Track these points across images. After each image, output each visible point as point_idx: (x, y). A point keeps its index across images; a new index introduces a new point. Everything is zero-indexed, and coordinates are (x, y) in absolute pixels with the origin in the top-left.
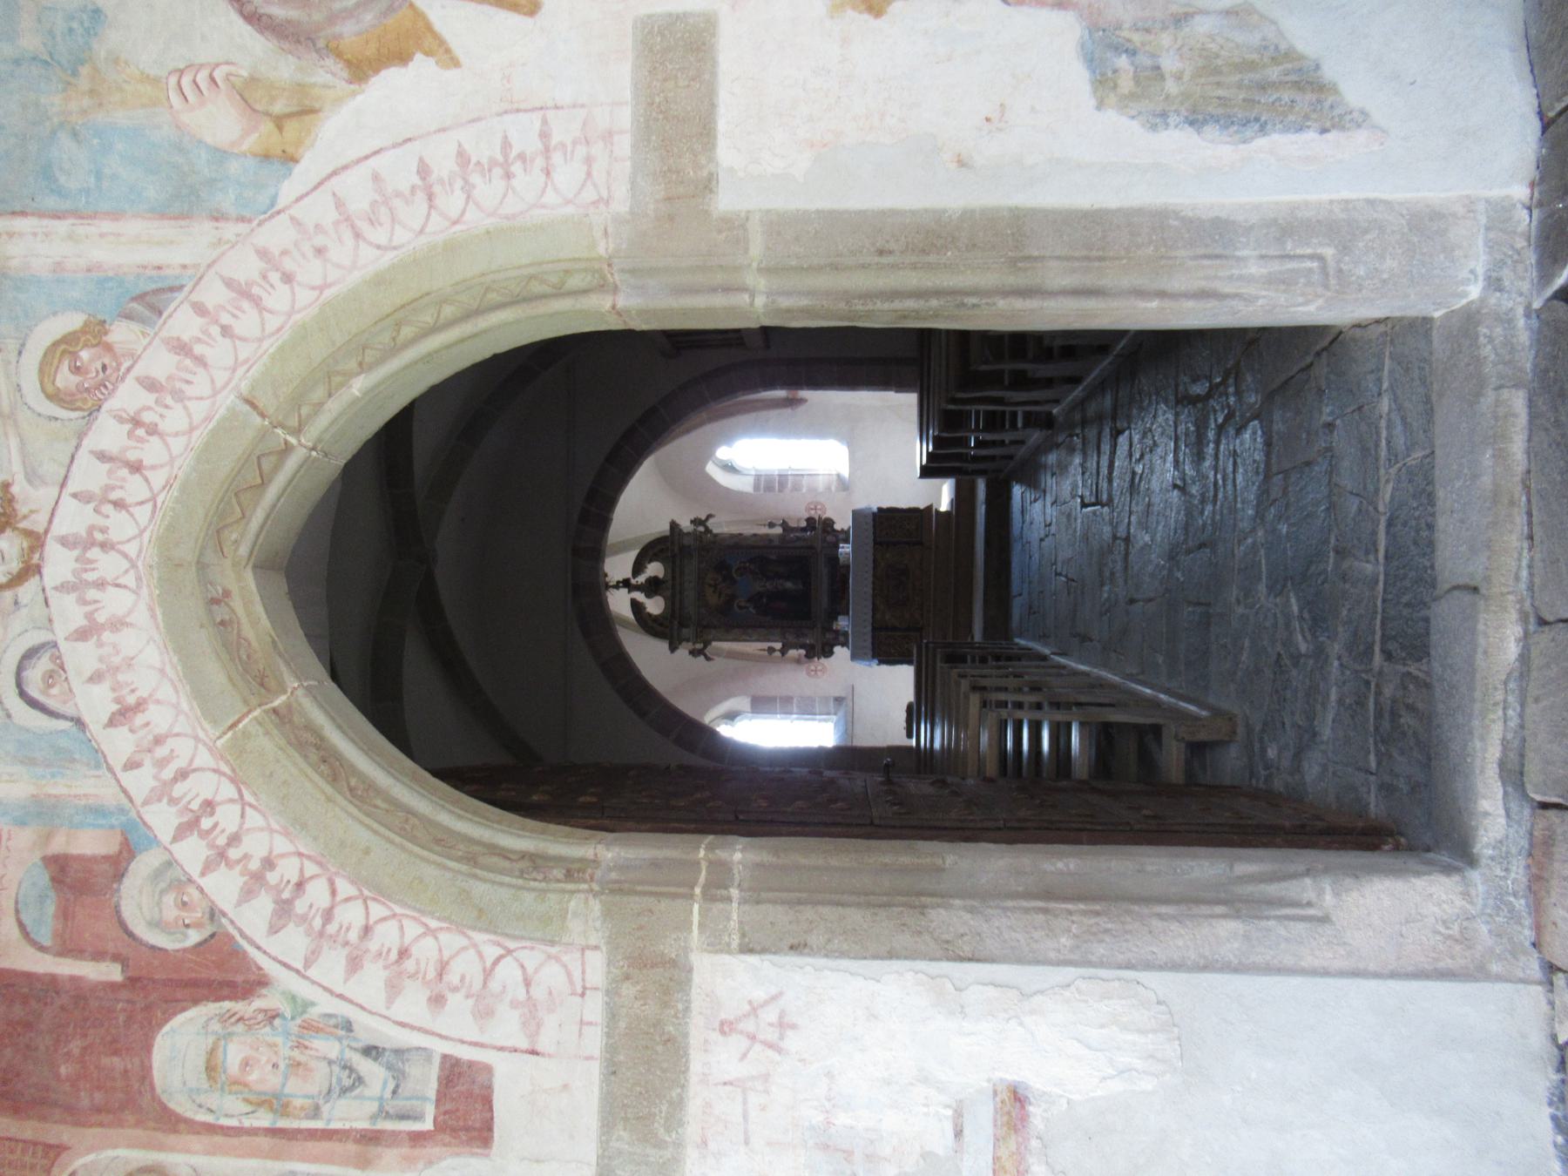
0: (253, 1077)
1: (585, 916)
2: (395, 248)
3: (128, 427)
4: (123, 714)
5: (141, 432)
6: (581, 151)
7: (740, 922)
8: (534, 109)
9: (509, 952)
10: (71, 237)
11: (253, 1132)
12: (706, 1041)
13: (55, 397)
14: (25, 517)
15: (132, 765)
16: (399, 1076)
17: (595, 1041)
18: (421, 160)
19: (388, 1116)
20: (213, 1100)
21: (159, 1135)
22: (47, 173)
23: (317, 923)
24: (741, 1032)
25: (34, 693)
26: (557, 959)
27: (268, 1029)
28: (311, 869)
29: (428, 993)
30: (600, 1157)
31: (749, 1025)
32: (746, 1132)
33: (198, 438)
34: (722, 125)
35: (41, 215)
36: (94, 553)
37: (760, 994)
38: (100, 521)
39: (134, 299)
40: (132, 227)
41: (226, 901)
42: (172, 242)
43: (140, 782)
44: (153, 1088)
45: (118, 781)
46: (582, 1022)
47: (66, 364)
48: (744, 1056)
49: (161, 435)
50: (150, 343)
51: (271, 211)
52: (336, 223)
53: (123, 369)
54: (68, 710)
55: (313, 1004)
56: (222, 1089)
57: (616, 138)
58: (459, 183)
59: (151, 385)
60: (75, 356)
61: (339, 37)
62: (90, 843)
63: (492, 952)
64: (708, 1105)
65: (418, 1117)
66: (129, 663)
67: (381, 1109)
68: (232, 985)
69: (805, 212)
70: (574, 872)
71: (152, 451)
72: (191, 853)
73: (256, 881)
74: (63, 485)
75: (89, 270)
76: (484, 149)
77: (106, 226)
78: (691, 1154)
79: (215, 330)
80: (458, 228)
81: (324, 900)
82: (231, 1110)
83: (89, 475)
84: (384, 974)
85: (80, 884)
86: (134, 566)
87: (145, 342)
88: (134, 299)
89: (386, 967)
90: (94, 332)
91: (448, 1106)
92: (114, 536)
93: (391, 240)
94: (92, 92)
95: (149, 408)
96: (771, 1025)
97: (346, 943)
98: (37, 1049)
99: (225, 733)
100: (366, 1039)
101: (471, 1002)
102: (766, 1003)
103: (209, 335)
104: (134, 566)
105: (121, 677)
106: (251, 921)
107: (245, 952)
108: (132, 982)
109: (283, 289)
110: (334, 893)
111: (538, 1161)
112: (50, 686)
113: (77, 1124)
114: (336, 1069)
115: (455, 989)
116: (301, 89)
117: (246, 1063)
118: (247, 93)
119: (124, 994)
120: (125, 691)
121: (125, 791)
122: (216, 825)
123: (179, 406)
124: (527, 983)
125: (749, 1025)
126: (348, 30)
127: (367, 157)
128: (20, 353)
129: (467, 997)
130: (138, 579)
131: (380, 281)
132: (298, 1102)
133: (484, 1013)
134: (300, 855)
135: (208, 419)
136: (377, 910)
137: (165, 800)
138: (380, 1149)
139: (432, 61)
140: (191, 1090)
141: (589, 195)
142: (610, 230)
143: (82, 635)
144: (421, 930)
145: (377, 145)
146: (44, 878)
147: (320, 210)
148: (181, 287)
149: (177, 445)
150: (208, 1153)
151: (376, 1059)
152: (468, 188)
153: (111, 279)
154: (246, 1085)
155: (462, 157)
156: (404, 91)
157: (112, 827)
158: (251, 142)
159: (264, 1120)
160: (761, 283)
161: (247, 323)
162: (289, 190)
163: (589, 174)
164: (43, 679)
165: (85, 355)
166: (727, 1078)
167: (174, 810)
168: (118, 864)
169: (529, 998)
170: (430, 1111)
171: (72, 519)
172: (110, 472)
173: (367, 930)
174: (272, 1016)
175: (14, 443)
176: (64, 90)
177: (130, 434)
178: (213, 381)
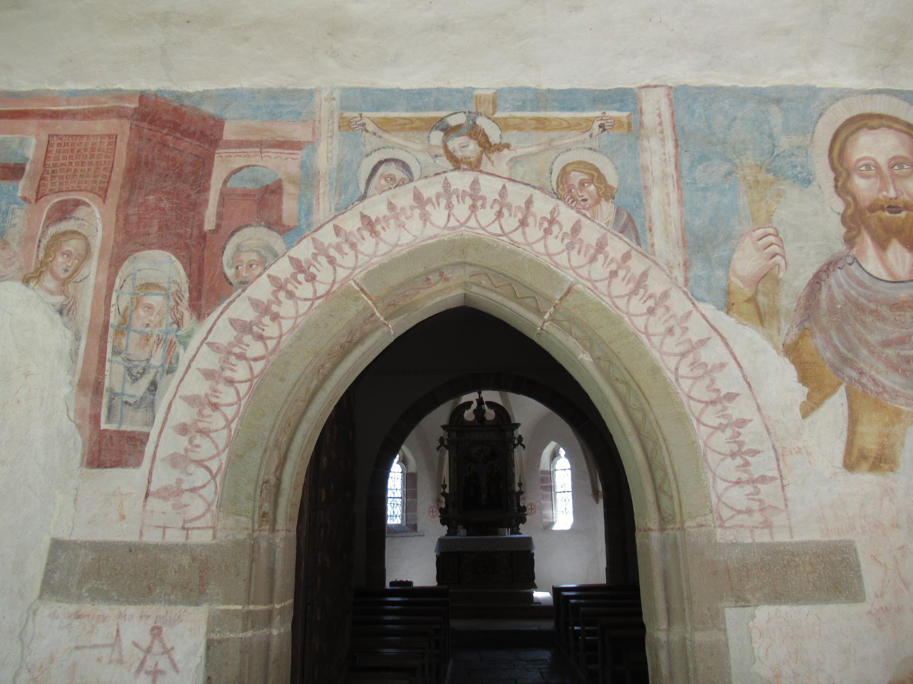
0: (141, 312)
1: (236, 528)
2: (677, 380)
3: (549, 217)
5: (546, 225)
6: (755, 506)
7: (228, 640)
8: (780, 471)
9: (214, 477)
10: (665, 175)
11: (107, 313)
12: (148, 617)
13: (564, 172)
14: (489, 158)
15: (337, 230)
16: (137, 405)
17: (153, 537)
18: (737, 395)
19: (111, 400)
20: (128, 288)
21: (108, 256)
22: (703, 158)
23: (237, 350)
24: (152, 642)
25: (382, 169)
26: (208, 510)
27: (171, 320)
28: (271, 344)
29: (189, 423)
30: (75, 543)
31: (157, 648)
32: (84, 647)
34: (784, 608)
35: (677, 156)
36: (469, 201)
37: (178, 656)
38: (488, 204)
39: (629, 216)
40: (674, 212)
42: (667, 237)
43: (327, 236)
44: (137, 251)
45: (328, 222)
46: (165, 528)
47: (586, 177)
48: (136, 645)
49: (544, 238)
50: (602, 227)
51: (694, 299)
52: (690, 341)
53: (584, 212)
54: (371, 191)
55: (185, 348)
56: (134, 294)
57: (766, 531)
58: (724, 421)
59: (576, 229)
60: (591, 182)
61: (813, 336)
62: (289, 207)
63: (214, 465)
64: (104, 619)
65: (109, 420)
66: (402, 226)
67: (116, 394)
68: (199, 298)
69: (729, 674)
70: (268, 518)
71: (534, 232)
72: (282, 269)
74: (510, 179)
75: (645, 187)
76: (751, 435)
77: (674, 197)
78: (72, 608)
79: (614, 267)
80: (695, 422)
81: (250, 354)
82: (121, 300)
83: (517, 195)
84: (203, 394)
85: (265, 203)
86: (462, 225)
87: (603, 224)
88: (629, 216)
89: (206, 395)
90: (606, 193)
91: (115, 439)
92: (480, 212)
93: (682, 377)
94: (757, 182)
95: (561, 229)
96: (156, 664)
97: (223, 369)
98: (165, 181)
99: (358, 285)
100: (161, 384)
101: (182, 452)
102: (172, 661)
103: (610, 264)
104: (462, 225)
105: (392, 221)
106: (240, 308)
107: (219, 305)
108: (203, 237)
109: (644, 308)
110: (256, 360)
111: (75, 500)
112: (386, 179)
113: (118, 207)
114: (143, 364)
115: (191, 441)
116: (775, 313)
117: (150, 307)
118: (768, 278)
119: (196, 232)
120: (384, 224)
121: (321, 227)
122: (300, 283)
123: (563, 247)
124: (193, 490)
125: (157, 648)
126: (818, 341)
127: (735, 358)
128: (590, 149)
129: (186, 450)
130: (454, 228)
131: (655, 371)
132: (124, 341)
133: (174, 461)
134: (280, 337)
135: (557, 265)
136: (243, 388)
137: (315, 251)
138: (90, 395)
139: (805, 399)
140: (135, 274)
141: (726, 513)
142: (703, 529)
143: (418, 197)
144: (230, 418)
145: (744, 364)
146: (268, 181)
148: (639, 244)
149: (539, 247)
150: (96, 285)
151: (148, 389)
152: (721, 428)
153: (641, 200)
154: (136, 308)
155: (742, 423)
156: (781, 382)
157: (299, 220)
158: (736, 282)
159: (114, 319)
160: (675, 638)
161: (620, 287)
162: (708, 309)
163: (739, 512)
164: (390, 175)
165: (592, 188)
166: (122, 632)
167: (310, 257)
168: (276, 225)
169: (183, 491)
170: (113, 427)
171: (490, 187)
172: (519, 208)
173: (231, 382)
174: (178, 323)
175: (534, 149)
176: (757, 165)
177: (544, 218)
178: (581, 267)
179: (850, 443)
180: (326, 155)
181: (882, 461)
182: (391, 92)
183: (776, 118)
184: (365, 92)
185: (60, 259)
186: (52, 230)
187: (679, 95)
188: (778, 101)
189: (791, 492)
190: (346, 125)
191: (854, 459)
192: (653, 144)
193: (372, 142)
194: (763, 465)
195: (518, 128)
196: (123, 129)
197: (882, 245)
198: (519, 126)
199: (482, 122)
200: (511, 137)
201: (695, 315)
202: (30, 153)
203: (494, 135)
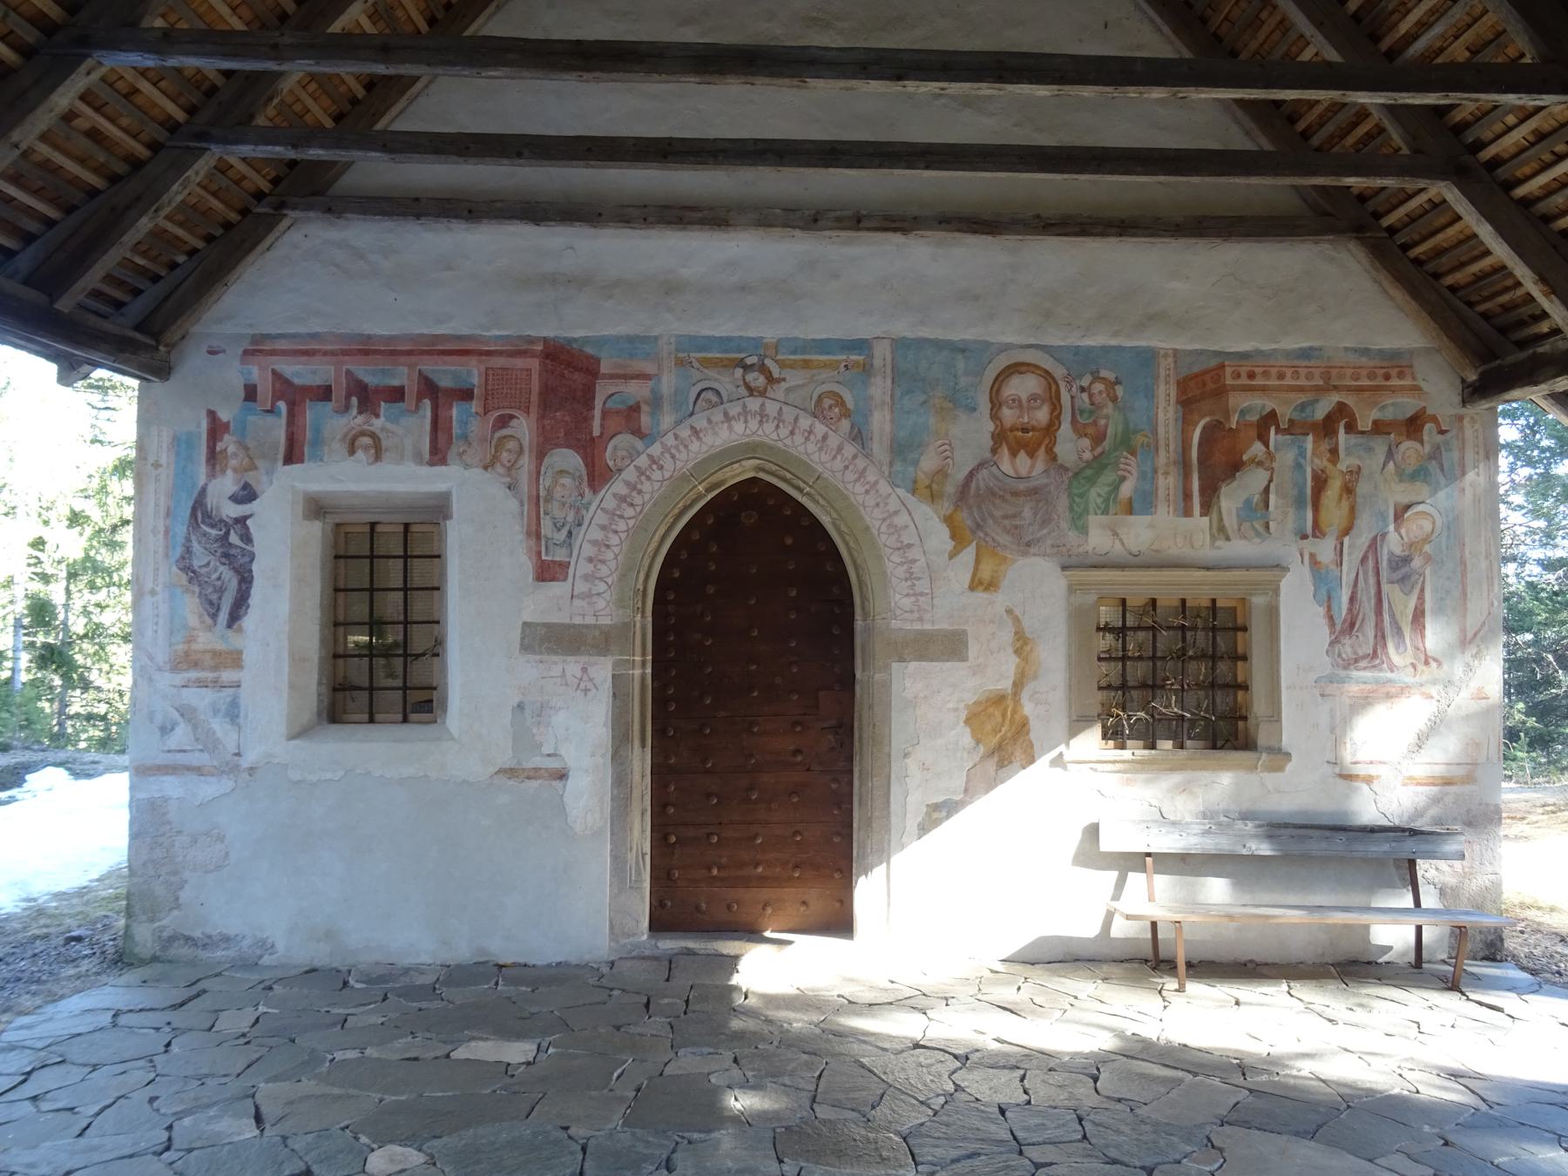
4: (696, 432)
10: (883, 403)
13: (820, 398)
15: (676, 437)
17: (577, 620)
20: (550, 473)
33: (804, 457)
40: (888, 427)
41: (624, 475)
43: (670, 440)
51: (894, 485)
59: (825, 438)
62: (645, 420)
63: (610, 581)
71: (799, 439)
72: (643, 461)
73: (632, 487)
76: (916, 569)
77: (888, 417)
82: (546, 481)
90: (846, 414)
106: (618, 487)
108: (593, 439)
118: (942, 473)
131: (867, 528)
133: (586, 578)
136: (623, 536)
141: (898, 612)
143: (726, 414)
146: (631, 403)
147: (894, 504)
149: (801, 449)
152: (902, 564)
155: (914, 561)
156: (940, 537)
159: (542, 493)
161: (850, 476)
162: (901, 492)
168: (637, 432)
174: (582, 495)
179: (974, 575)
180: (668, 382)
181: (991, 586)
182: (709, 338)
183: (961, 364)
184: (692, 338)
185: (505, 454)
186: (497, 435)
187: (900, 345)
188: (963, 351)
189: (936, 601)
190: (680, 363)
191: (976, 584)
192: (877, 380)
193: (696, 375)
194: (924, 586)
195: (792, 367)
196: (534, 364)
197: (1014, 454)
198: (792, 366)
199: (768, 362)
200: (787, 373)
201: (894, 496)
202: (475, 381)
203: (776, 375)
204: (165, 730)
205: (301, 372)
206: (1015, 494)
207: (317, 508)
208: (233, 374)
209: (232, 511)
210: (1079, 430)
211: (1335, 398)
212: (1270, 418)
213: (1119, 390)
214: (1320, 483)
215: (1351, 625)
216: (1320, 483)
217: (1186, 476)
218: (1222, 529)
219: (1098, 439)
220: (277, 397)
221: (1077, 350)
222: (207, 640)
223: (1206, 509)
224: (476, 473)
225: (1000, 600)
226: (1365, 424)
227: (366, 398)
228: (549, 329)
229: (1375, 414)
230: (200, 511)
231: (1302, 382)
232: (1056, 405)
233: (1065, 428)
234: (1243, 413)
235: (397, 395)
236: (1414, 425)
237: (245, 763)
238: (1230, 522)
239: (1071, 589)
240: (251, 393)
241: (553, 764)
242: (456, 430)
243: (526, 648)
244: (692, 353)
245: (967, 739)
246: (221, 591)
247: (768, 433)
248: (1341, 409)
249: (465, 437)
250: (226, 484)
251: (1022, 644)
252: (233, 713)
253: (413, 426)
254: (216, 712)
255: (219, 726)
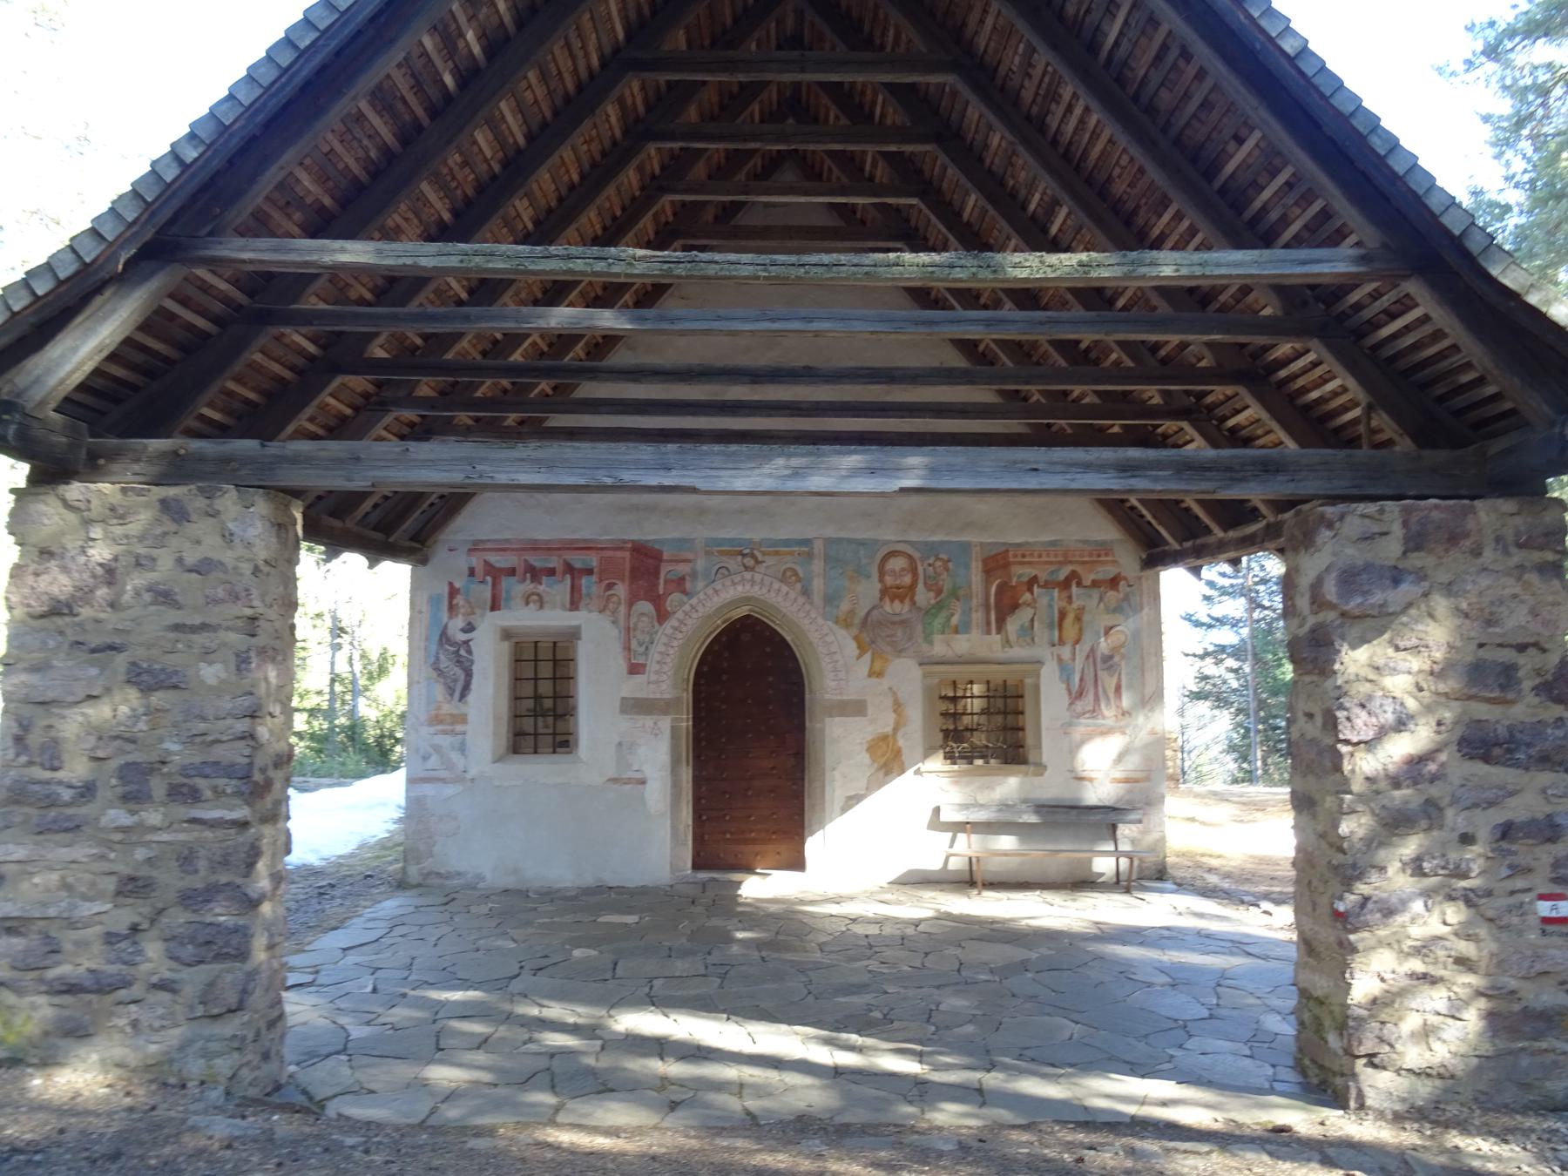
4: (716, 592)
43: (701, 596)
62: (688, 585)
71: (773, 594)
72: (687, 607)
73: (682, 622)
82: (633, 620)
83: (767, 580)
85: (679, 583)
90: (799, 580)
106: (673, 622)
118: (852, 612)
133: (657, 672)
156: (851, 648)
161: (802, 614)
168: (684, 592)
171: (758, 577)
180: (700, 564)
181: (880, 674)
184: (715, 540)
187: (830, 542)
190: (707, 553)
191: (871, 674)
194: (842, 675)
196: (627, 555)
197: (892, 601)
198: (769, 554)
200: (767, 558)
203: (760, 558)
204: (425, 758)
205: (498, 560)
206: (893, 623)
207: (507, 634)
208: (462, 562)
209: (462, 637)
210: (928, 588)
211: (1070, 568)
212: (1033, 580)
213: (950, 565)
214: (1063, 615)
215: (1080, 694)
216: (1063, 615)
217: (988, 613)
218: (1008, 641)
219: (939, 592)
220: (487, 573)
221: (926, 544)
222: (448, 708)
223: (999, 631)
224: (595, 615)
225: (885, 682)
226: (1087, 582)
227: (535, 574)
228: (635, 535)
229: (1092, 577)
230: (444, 637)
231: (1052, 559)
232: (914, 571)
233: (920, 587)
234: (1020, 576)
235: (551, 572)
236: (1114, 582)
237: (469, 776)
238: (1012, 637)
239: (925, 676)
240: (472, 572)
241: (638, 776)
242: (584, 591)
243: (623, 711)
244: (717, 548)
245: (866, 758)
246: (455, 681)
247: (756, 591)
248: (1074, 574)
249: (588, 595)
250: (459, 622)
251: (898, 707)
252: (462, 749)
253: (559, 590)
254: (453, 748)
255: (455, 756)
